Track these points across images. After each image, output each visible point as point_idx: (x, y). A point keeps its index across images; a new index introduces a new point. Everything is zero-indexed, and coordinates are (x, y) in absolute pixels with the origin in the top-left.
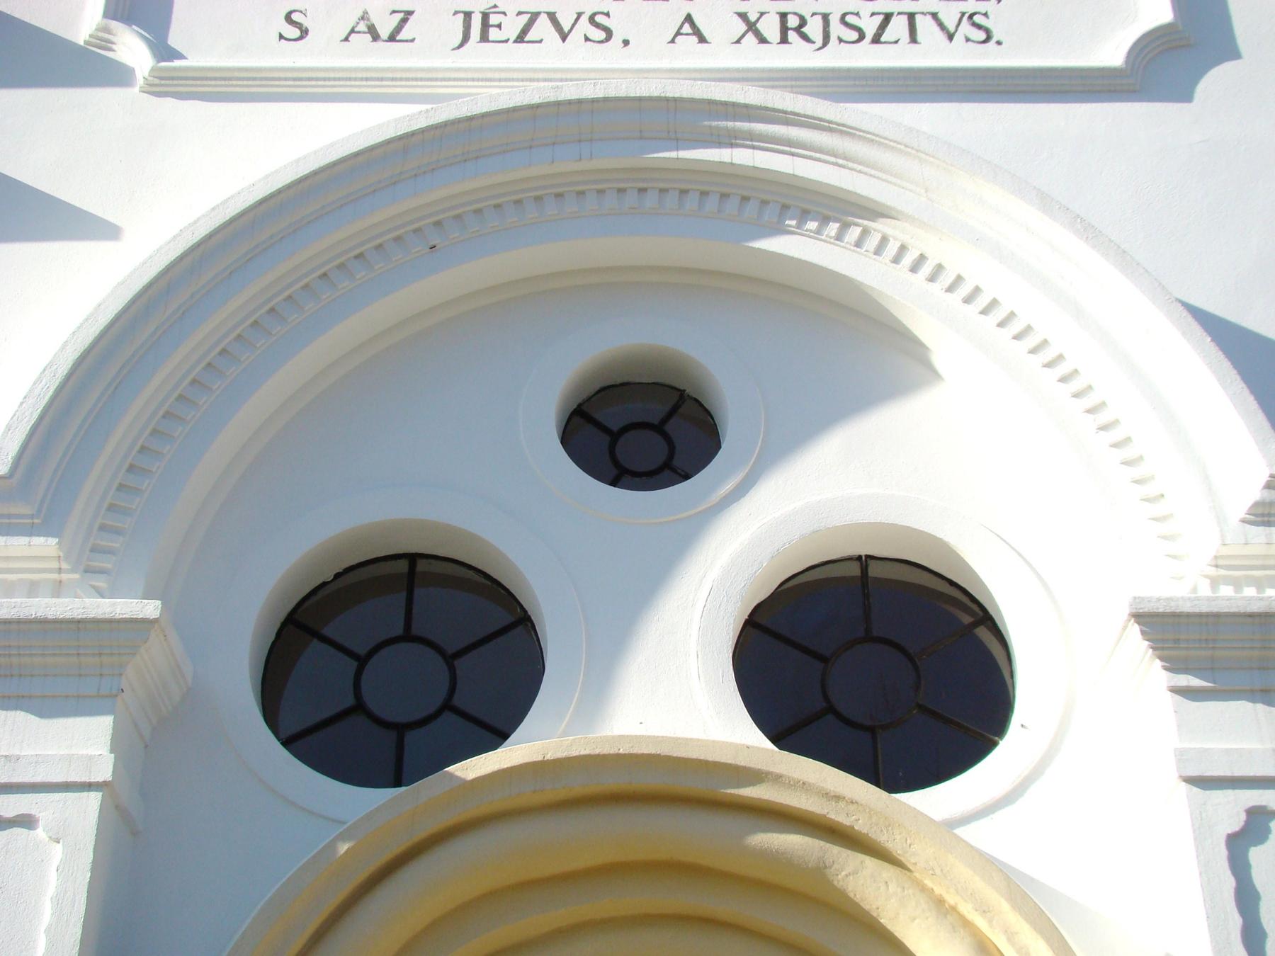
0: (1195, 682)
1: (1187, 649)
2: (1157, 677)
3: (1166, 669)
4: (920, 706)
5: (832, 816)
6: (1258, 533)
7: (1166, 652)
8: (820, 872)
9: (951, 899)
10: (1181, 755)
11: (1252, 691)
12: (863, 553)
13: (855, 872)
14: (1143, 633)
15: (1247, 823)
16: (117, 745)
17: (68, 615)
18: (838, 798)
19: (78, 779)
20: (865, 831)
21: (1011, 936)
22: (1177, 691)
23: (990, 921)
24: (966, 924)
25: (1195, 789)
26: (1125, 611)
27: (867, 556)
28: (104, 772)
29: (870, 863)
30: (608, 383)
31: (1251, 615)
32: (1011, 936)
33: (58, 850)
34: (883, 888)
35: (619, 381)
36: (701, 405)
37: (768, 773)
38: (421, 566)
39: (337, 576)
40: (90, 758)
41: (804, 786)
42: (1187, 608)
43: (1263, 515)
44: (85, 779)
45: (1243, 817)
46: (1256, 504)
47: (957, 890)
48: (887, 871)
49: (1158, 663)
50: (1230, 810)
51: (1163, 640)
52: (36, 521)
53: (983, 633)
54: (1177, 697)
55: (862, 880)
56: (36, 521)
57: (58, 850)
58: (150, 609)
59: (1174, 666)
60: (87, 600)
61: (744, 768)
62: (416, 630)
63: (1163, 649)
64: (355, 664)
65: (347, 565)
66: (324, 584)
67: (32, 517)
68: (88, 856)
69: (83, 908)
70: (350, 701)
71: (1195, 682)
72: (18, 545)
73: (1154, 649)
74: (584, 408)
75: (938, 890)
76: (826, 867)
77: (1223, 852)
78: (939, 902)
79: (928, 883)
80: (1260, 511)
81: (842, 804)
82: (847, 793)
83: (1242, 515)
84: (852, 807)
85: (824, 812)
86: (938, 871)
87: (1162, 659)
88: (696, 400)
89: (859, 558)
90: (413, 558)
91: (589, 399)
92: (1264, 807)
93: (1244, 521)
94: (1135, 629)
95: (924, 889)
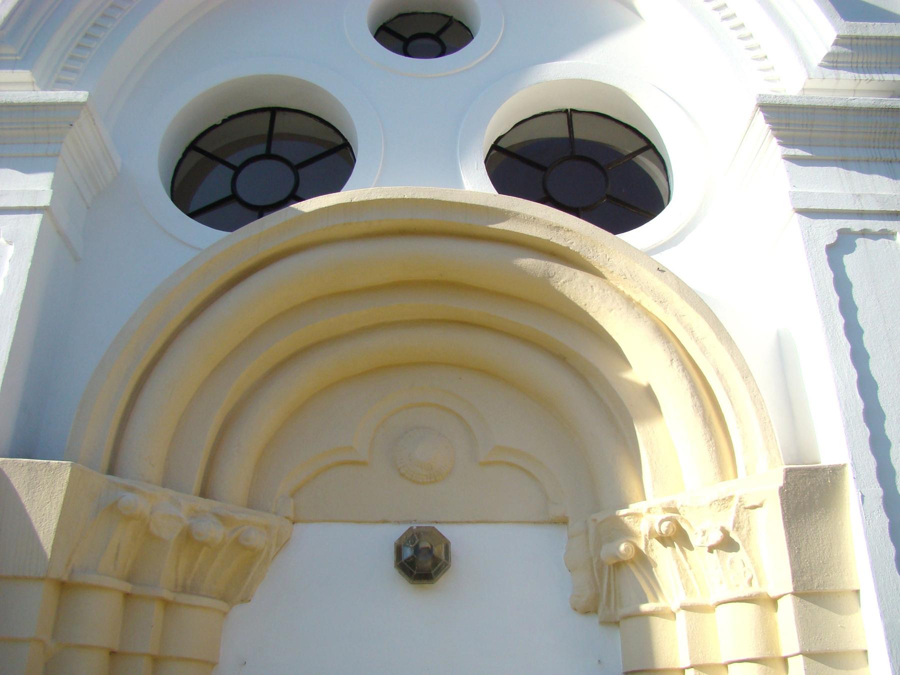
0: (799, 152)
1: (794, 130)
2: (775, 150)
3: (780, 144)
4: (608, 197)
5: (554, 240)
6: (830, 73)
7: (781, 133)
8: (545, 281)
9: (636, 298)
10: (794, 196)
11: (836, 160)
12: (569, 108)
13: (570, 280)
14: (765, 118)
15: (838, 239)
16: (55, 185)
17: (26, 101)
18: (558, 228)
19: (27, 205)
20: (577, 250)
21: (679, 317)
22: (788, 158)
23: (665, 309)
24: (644, 313)
25: (803, 217)
26: (754, 102)
27: (572, 110)
28: (45, 200)
29: (580, 275)
30: (402, 11)
31: (835, 109)
32: (679, 317)
33: (11, 250)
34: (589, 290)
35: (410, 11)
36: (463, 25)
37: (509, 212)
38: (283, 124)
39: (224, 121)
40: (37, 192)
41: (533, 220)
42: (794, 102)
43: (833, 62)
44: (32, 204)
45: (836, 235)
46: (829, 55)
47: (641, 288)
48: (592, 280)
49: (775, 140)
50: (828, 231)
51: (779, 124)
52: (18, 58)
53: (645, 162)
54: (788, 162)
55: (574, 286)
56: (18, 58)
57: (11, 250)
58: (81, 96)
59: (786, 142)
60: (40, 92)
61: (492, 208)
62: (273, 151)
63: (778, 130)
64: (231, 172)
65: (230, 114)
66: (215, 127)
67: (16, 55)
68: (30, 253)
69: (25, 285)
70: (229, 193)
71: (799, 152)
72: (6, 75)
73: (773, 129)
74: (388, 26)
75: (628, 292)
76: (550, 277)
77: (824, 256)
78: (629, 300)
79: (621, 287)
80: (831, 59)
81: (561, 232)
82: (565, 225)
83: (820, 62)
84: (568, 234)
85: (548, 238)
86: (628, 276)
87: (778, 137)
88: (460, 22)
89: (567, 110)
90: (273, 111)
91: (391, 21)
92: (849, 229)
93: (821, 65)
94: (760, 116)
95: (618, 291)
